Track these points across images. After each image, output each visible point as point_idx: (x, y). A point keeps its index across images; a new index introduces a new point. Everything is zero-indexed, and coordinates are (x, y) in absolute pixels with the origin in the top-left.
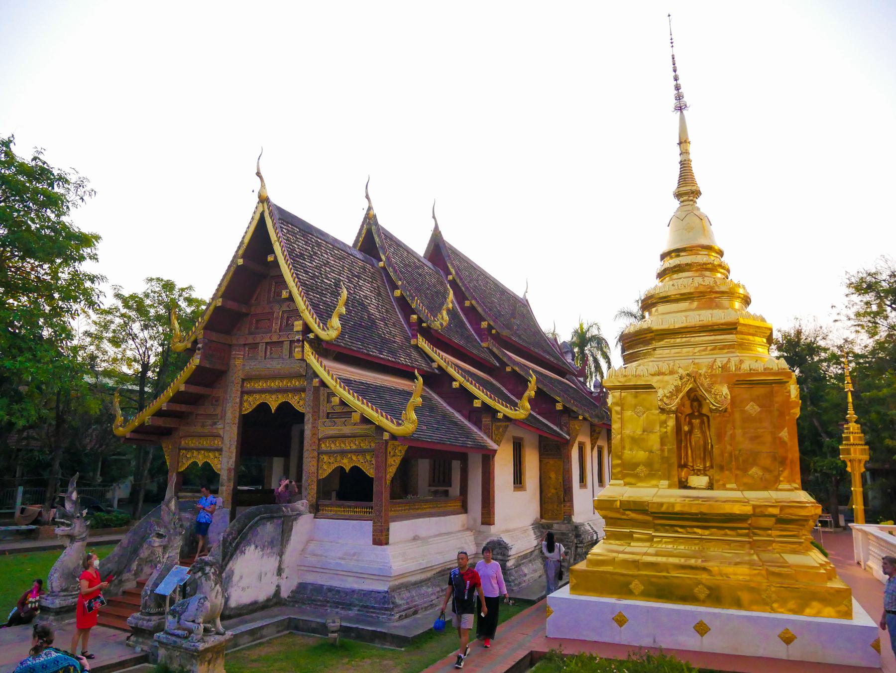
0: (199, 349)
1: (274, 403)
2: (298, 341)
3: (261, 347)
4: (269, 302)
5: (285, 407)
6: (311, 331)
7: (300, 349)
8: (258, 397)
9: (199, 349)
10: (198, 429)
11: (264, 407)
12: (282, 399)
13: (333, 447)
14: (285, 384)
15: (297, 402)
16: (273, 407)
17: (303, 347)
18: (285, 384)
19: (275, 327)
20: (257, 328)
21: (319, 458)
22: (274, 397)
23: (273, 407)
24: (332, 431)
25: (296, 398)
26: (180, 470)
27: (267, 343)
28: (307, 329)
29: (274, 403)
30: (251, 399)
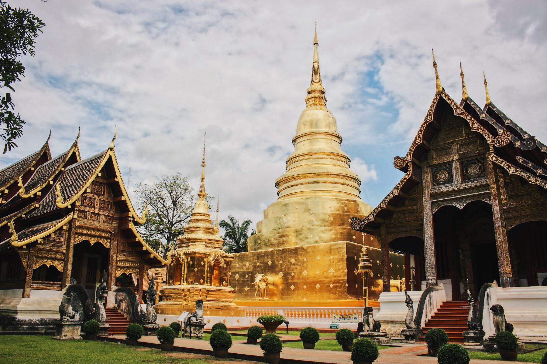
1: (93, 241)
9: (77, 210)
11: (86, 242)
12: (96, 240)
14: (98, 234)
19: (97, 206)
22: (93, 239)
24: (123, 258)
29: (93, 241)
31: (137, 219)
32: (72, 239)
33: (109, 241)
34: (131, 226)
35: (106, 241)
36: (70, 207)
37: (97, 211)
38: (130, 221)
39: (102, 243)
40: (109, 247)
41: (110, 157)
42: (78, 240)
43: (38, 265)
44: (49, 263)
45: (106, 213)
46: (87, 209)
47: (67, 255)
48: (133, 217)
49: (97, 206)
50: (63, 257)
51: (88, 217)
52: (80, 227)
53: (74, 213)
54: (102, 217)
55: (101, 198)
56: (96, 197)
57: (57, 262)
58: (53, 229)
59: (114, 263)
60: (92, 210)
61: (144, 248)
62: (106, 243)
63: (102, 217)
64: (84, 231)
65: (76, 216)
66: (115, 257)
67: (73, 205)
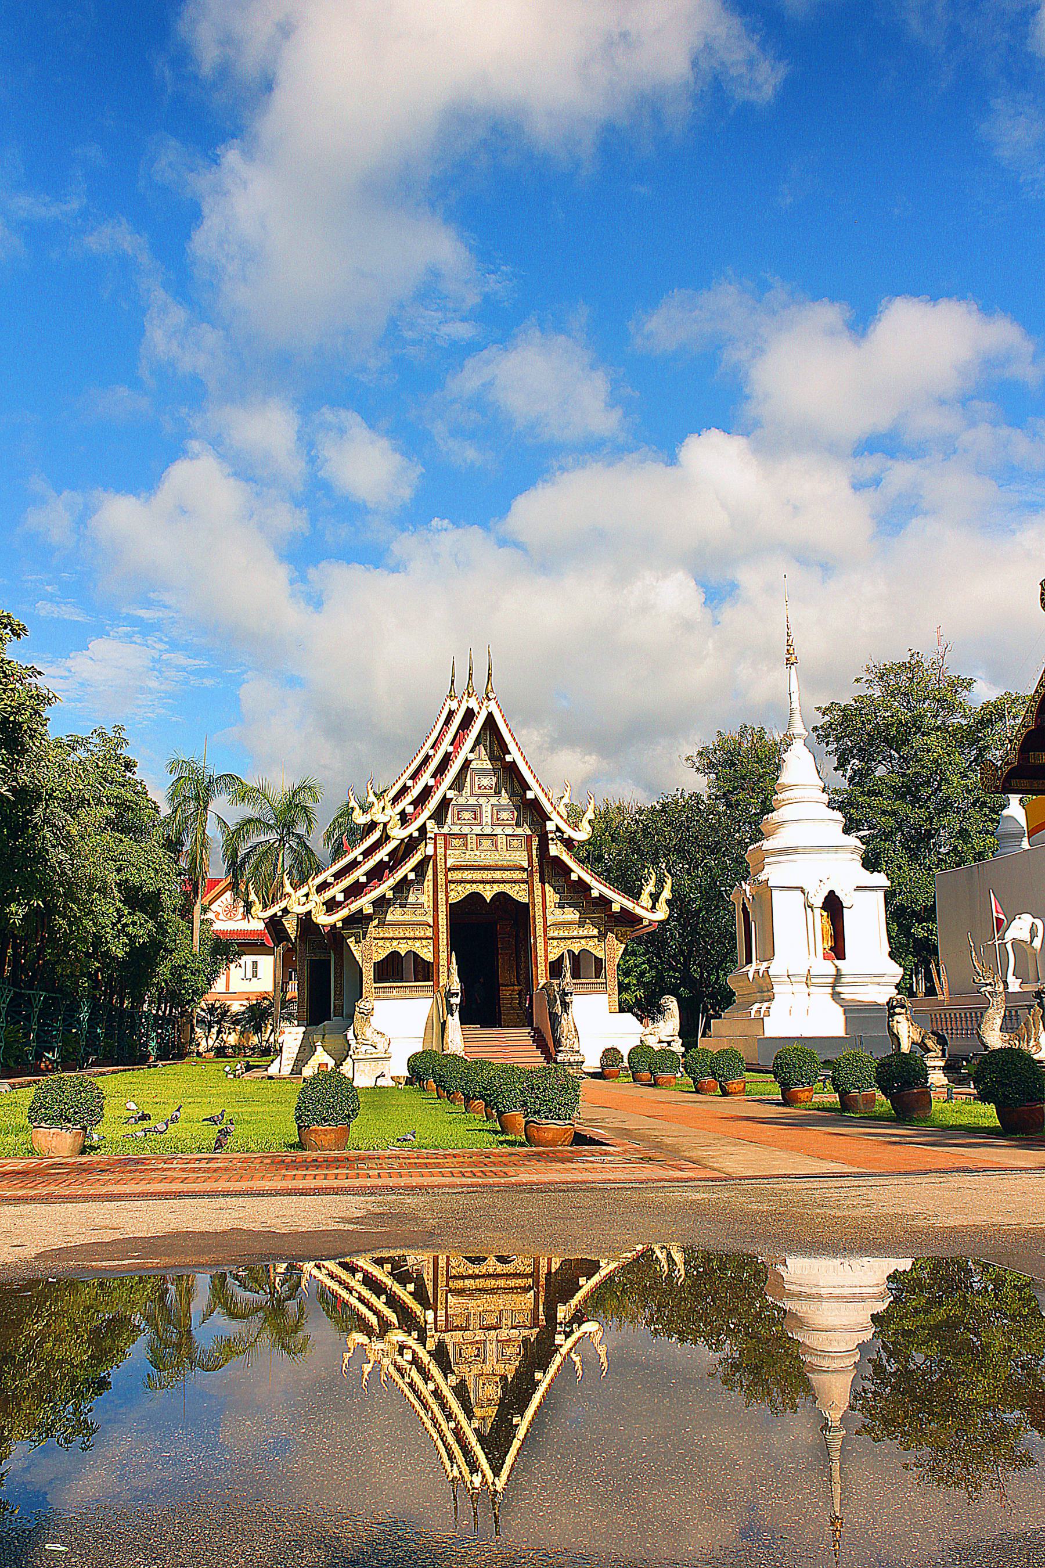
1: (488, 893)
3: (472, 840)
5: (501, 896)
6: (563, 833)
8: (468, 886)
11: (475, 896)
12: (497, 888)
13: (562, 934)
14: (498, 875)
16: (488, 896)
18: (498, 875)
19: (487, 819)
22: (488, 886)
23: (488, 896)
29: (488, 893)
30: (459, 888)
31: (569, 832)
32: (441, 896)
33: (524, 886)
34: (555, 850)
35: (517, 887)
36: (416, 834)
37: (488, 831)
38: (553, 839)
39: (511, 893)
41: (490, 715)
42: (458, 893)
43: (383, 955)
46: (466, 830)
47: (435, 926)
48: (558, 829)
49: (487, 819)
50: (429, 933)
51: (469, 847)
56: (482, 800)
57: (418, 943)
58: (391, 882)
59: (540, 932)
60: (477, 830)
61: (595, 893)
62: (518, 893)
63: (502, 840)
64: (468, 875)
65: (430, 851)
66: (539, 920)
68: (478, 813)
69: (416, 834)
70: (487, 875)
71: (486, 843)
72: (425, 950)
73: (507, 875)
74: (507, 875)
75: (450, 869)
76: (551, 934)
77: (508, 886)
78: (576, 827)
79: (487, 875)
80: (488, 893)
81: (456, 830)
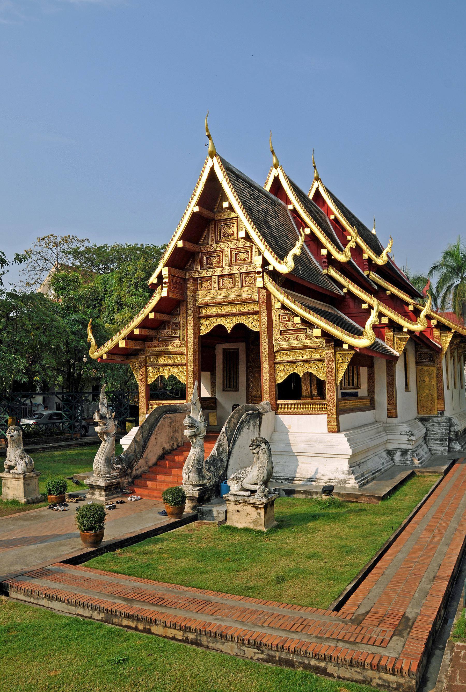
0: (165, 283)
2: (259, 272)
4: (217, 242)
5: (240, 327)
7: (261, 279)
8: (214, 320)
9: (165, 283)
10: (156, 349)
11: (220, 329)
12: (235, 321)
13: (288, 359)
14: (237, 309)
15: (250, 323)
17: (263, 277)
18: (237, 309)
19: (226, 261)
20: (207, 264)
21: (275, 367)
22: (229, 320)
25: (250, 319)
26: (150, 382)
27: (219, 276)
28: (265, 263)
29: (229, 325)
30: (207, 322)
37: (227, 272)
40: (257, 330)
44: (166, 373)
45: (243, 270)
46: (210, 274)
51: (213, 286)
52: (205, 306)
53: (162, 288)
54: (237, 278)
55: (233, 245)
60: (219, 272)
67: (160, 277)
68: (221, 257)
69: (155, 281)
70: (229, 309)
71: (227, 281)
72: (181, 375)
73: (244, 308)
74: (244, 308)
75: (199, 307)
76: (278, 359)
77: (244, 318)
78: (281, 256)
79: (229, 309)
80: (229, 325)
81: (204, 274)
